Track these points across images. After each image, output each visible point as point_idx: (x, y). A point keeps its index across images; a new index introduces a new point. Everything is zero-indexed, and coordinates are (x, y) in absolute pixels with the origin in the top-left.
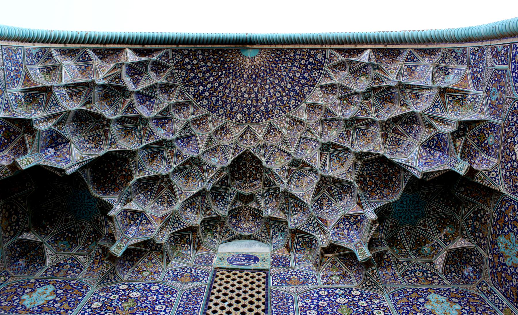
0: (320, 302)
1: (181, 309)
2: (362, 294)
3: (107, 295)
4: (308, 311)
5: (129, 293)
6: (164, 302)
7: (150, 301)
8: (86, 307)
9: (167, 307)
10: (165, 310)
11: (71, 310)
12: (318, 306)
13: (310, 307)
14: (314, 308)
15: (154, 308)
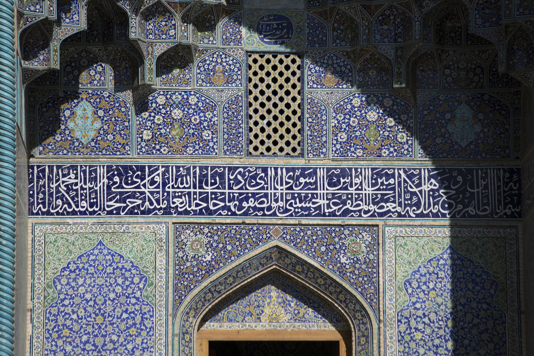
0: (352, 119)
1: (226, 136)
2: (393, 105)
3: (150, 116)
4: (339, 135)
5: (171, 111)
6: (208, 126)
7: (194, 125)
8: (139, 139)
9: (213, 134)
10: (212, 138)
11: (127, 145)
12: (349, 125)
13: (341, 128)
14: (345, 129)
15: (202, 137)
